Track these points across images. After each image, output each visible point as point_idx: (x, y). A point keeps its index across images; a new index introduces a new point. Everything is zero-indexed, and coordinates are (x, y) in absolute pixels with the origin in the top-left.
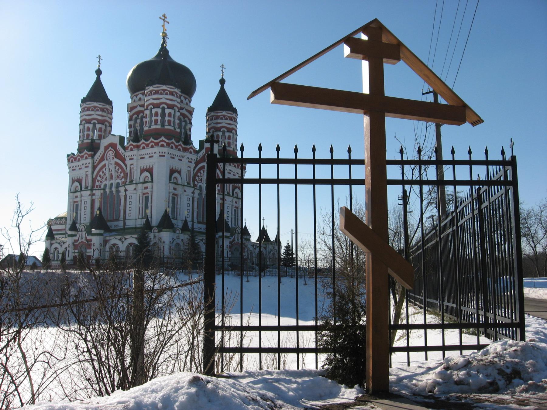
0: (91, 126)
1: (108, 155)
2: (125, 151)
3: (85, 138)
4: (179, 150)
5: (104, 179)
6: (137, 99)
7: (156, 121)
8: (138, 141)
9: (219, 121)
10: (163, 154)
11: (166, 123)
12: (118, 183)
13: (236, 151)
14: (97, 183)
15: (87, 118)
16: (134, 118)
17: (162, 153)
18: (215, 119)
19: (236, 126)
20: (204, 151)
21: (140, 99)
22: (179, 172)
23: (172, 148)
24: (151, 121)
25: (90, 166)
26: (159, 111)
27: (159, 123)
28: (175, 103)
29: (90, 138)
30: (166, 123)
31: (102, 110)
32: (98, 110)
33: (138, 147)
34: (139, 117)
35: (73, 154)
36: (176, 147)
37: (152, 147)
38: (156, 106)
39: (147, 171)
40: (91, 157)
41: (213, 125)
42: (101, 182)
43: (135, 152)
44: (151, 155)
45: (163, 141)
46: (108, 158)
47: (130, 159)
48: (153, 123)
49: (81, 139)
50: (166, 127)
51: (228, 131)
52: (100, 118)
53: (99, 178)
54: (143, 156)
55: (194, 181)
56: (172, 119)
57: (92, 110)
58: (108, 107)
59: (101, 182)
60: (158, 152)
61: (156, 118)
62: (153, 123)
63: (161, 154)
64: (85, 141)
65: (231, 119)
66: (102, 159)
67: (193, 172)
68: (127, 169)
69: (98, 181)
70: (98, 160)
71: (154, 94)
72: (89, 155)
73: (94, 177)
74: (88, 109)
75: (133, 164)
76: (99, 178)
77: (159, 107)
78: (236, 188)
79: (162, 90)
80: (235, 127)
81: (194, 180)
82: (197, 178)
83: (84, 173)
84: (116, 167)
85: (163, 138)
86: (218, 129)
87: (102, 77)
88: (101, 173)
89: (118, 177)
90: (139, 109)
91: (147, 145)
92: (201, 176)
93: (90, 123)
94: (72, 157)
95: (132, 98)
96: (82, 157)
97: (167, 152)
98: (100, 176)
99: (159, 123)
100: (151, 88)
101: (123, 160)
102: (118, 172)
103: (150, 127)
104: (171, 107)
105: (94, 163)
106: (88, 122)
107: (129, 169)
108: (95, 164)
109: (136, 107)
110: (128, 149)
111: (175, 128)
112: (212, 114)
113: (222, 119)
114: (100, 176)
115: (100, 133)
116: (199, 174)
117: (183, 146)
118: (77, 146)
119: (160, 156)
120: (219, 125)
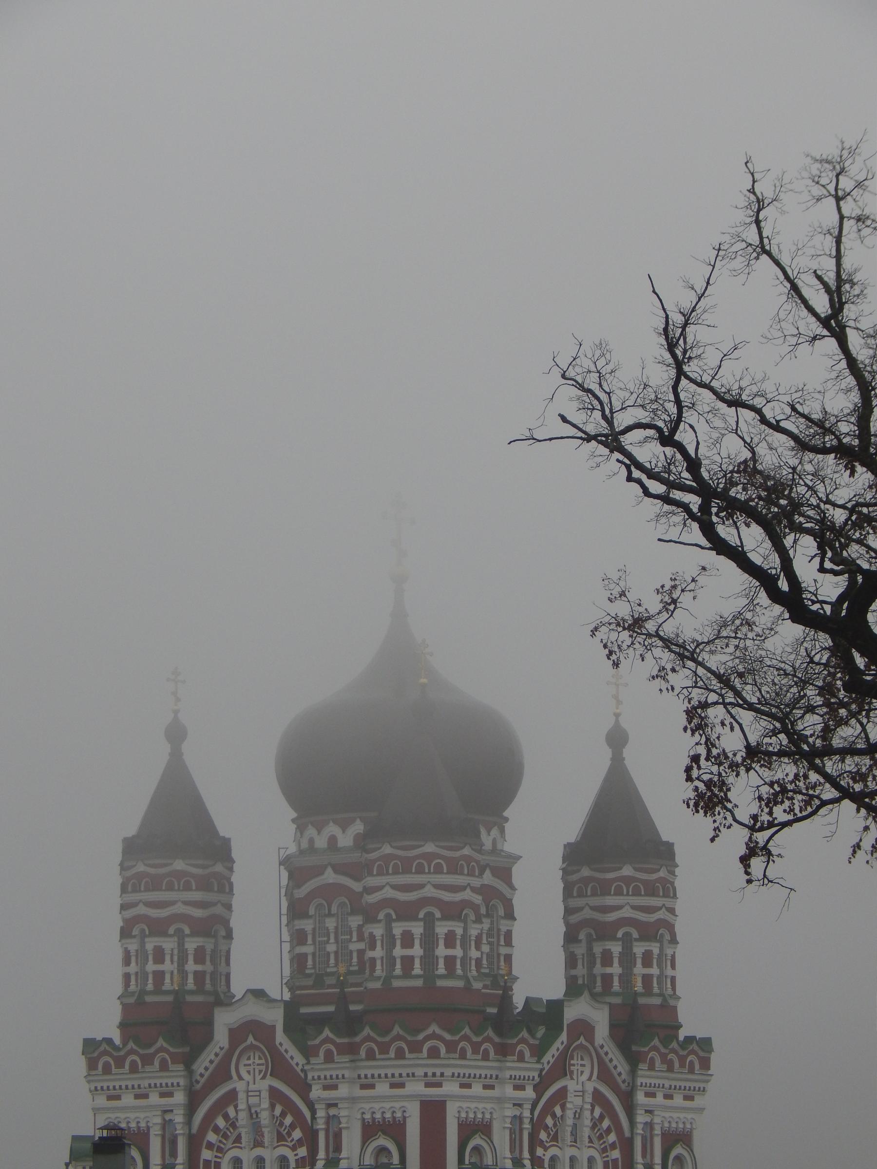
0: (169, 944)
1: (244, 1061)
2: (307, 1058)
3: (150, 987)
4: (486, 1057)
5: (232, 1138)
6: (321, 842)
7: (408, 962)
8: (353, 1033)
9: (610, 901)
10: (438, 1079)
11: (441, 970)
12: (283, 1159)
13: (672, 1002)
14: (206, 1154)
15: (154, 913)
16: (312, 912)
17: (434, 1075)
18: (594, 894)
19: (672, 911)
20: (564, 1037)
21: (333, 840)
22: (485, 1128)
23: (463, 1056)
24: (390, 961)
25: (180, 1097)
26: (417, 929)
27: (417, 970)
28: (467, 895)
29: (167, 985)
30: (441, 970)
31: (204, 884)
32: (187, 888)
33: (351, 1049)
34: (334, 910)
35: (109, 1041)
36: (476, 1048)
37: (400, 1055)
38: (406, 912)
39: (385, 1133)
40: (181, 1067)
41: (587, 913)
42: (220, 1150)
43: (342, 1067)
44: (397, 1079)
45: (434, 1036)
46: (243, 1072)
47: (326, 1088)
48: (398, 971)
49: (133, 987)
50: (440, 983)
51: (643, 938)
52: (198, 913)
53: (212, 1137)
54: (370, 1081)
55: (532, 1151)
56: (458, 952)
57: (170, 888)
58: (219, 868)
59: (220, 1150)
60: (420, 1072)
61: (408, 952)
62: (398, 971)
63: (430, 1079)
64: (149, 999)
65: (652, 892)
66: (222, 1073)
67: (532, 1119)
68: (313, 1118)
69: (210, 1146)
70: (207, 1074)
71: (396, 872)
72: (175, 1059)
73: (195, 1130)
74: (155, 884)
75: (336, 1105)
76: (212, 1137)
77: (414, 918)
78: (676, 1142)
79: (424, 856)
80: (668, 917)
81: (534, 1142)
82: (543, 1136)
83: (159, 1120)
84: (272, 1106)
85: (434, 1028)
86: (604, 932)
87: (186, 747)
88: (221, 1122)
89: (280, 1138)
90: (330, 877)
91: (384, 1049)
92: (555, 1125)
93: (164, 934)
94: (105, 1053)
95: (301, 829)
96: (147, 1060)
97: (448, 1072)
98: (216, 1130)
99: (417, 970)
100: (387, 849)
101: (304, 1089)
102: (281, 1124)
103: (387, 980)
104: (453, 912)
105: (192, 1085)
106: (158, 928)
107: (321, 1125)
108: (198, 1087)
109: (319, 871)
110: (317, 1055)
111: (468, 981)
112: (586, 872)
113: (619, 892)
114: (216, 1130)
115: (199, 968)
116: (549, 1121)
117: (497, 1040)
118: (115, 1014)
119: (428, 1085)
120: (612, 917)
